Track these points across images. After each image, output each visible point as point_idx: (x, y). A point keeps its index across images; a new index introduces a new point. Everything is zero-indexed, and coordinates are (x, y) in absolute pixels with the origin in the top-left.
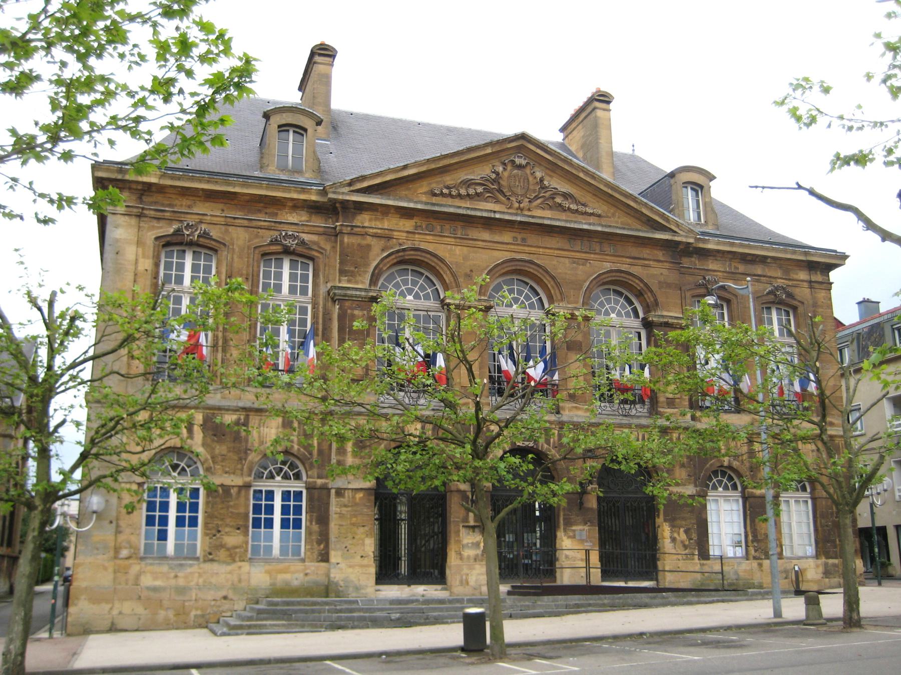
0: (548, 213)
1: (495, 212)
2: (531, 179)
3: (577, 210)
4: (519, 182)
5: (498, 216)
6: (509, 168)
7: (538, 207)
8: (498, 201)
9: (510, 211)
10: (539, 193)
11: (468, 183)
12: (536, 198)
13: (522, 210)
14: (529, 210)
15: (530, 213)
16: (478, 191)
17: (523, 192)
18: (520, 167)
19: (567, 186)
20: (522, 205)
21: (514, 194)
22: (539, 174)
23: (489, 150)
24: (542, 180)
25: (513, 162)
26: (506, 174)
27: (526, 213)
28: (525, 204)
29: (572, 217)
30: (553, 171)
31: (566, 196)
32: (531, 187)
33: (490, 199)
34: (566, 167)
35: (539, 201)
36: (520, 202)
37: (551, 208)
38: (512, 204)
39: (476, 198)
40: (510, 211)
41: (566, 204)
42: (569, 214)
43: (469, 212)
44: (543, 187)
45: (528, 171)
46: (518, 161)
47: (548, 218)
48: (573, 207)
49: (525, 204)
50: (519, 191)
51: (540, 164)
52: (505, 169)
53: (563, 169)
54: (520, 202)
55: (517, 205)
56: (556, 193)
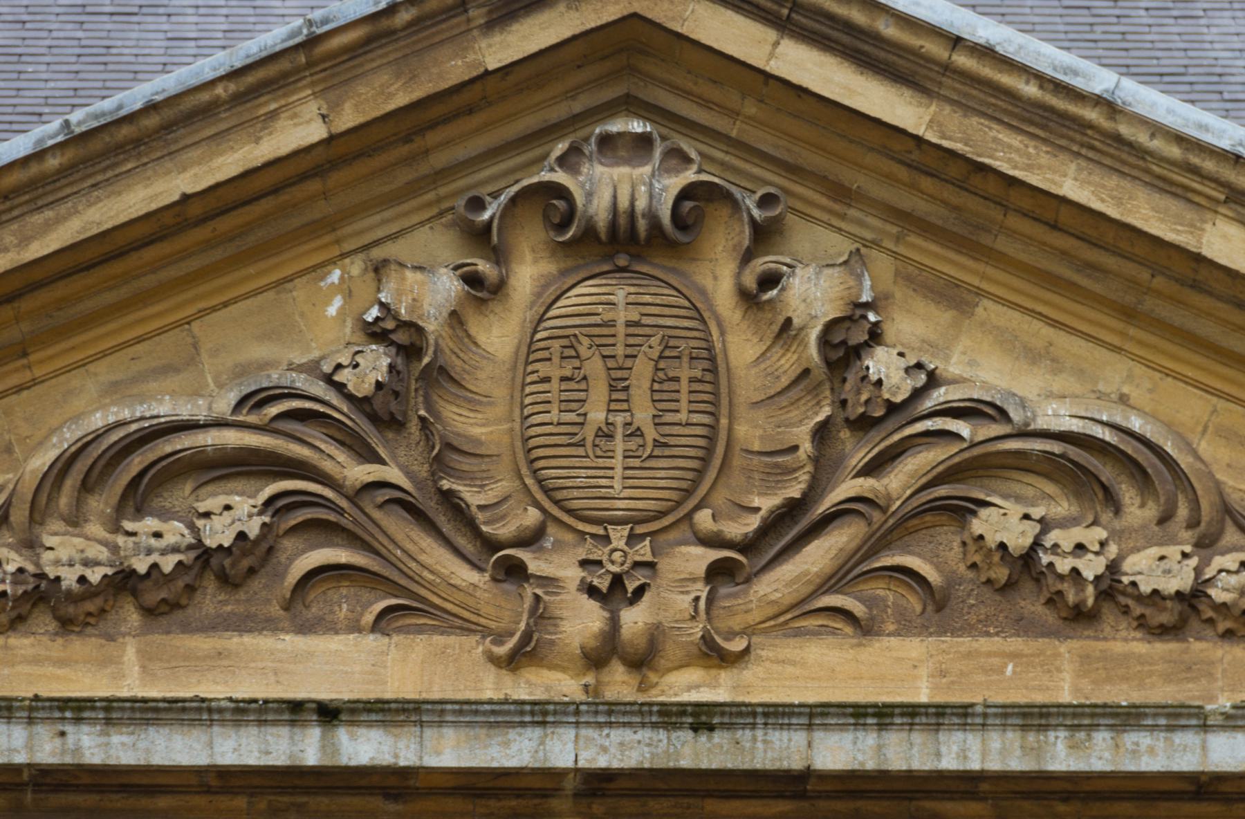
0: (906, 666)
1: (329, 714)
2: (743, 347)
3: (1192, 599)
4: (618, 388)
5: (364, 747)
6: (528, 273)
7: (800, 615)
8: (407, 608)
9: (529, 686)
10: (824, 469)
11: (137, 469)
12: (790, 526)
13: (643, 660)
14: (713, 654)
15: (716, 689)
16: (219, 533)
17: (663, 479)
18: (624, 244)
19: (1116, 373)
20: (634, 619)
21: (561, 512)
22: (813, 294)
23: (299, 128)
24: (846, 344)
25: (551, 203)
26: (498, 336)
27: (687, 685)
28: (674, 595)
29: (1130, 664)
30: (966, 243)
31: (1089, 468)
32: (750, 431)
33: (338, 601)
34: (1073, 183)
35: (819, 556)
36: (614, 593)
37: (938, 607)
38: (541, 615)
39: (211, 600)
40: (529, 686)
41: (1082, 548)
42: (1126, 643)
43: (93, 746)
44: (883, 422)
45: (718, 275)
46: (609, 186)
47: (860, 715)
48: (1158, 568)
49: (674, 595)
50: (620, 486)
51: (842, 193)
52: (482, 290)
53: (1052, 211)
54: (614, 593)
55: (582, 621)
56: (1003, 454)
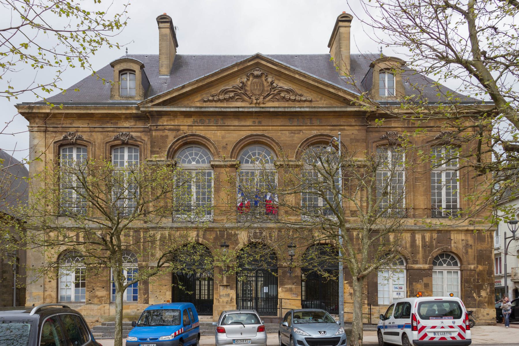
0: (276, 104)
1: (238, 107)
2: (265, 83)
3: (295, 100)
4: (257, 86)
5: (241, 110)
6: (251, 79)
7: (269, 101)
8: (243, 101)
10: (271, 91)
11: (225, 92)
12: (268, 95)
13: (259, 104)
14: (263, 103)
15: (264, 106)
16: (231, 96)
17: (260, 92)
18: (257, 77)
19: (290, 85)
20: (258, 101)
21: (253, 94)
22: (270, 80)
24: (272, 83)
26: (249, 83)
27: (262, 105)
28: (261, 100)
29: (291, 104)
31: (288, 91)
32: (266, 89)
34: (287, 72)
35: (270, 97)
36: (257, 100)
37: (278, 100)
38: (252, 101)
39: (231, 100)
41: (287, 96)
43: (223, 110)
45: (263, 79)
46: (256, 73)
47: (273, 107)
48: (293, 98)
49: (261, 100)
50: (257, 92)
51: (272, 73)
52: (248, 80)
54: (257, 100)
55: (255, 101)
56: (282, 90)
